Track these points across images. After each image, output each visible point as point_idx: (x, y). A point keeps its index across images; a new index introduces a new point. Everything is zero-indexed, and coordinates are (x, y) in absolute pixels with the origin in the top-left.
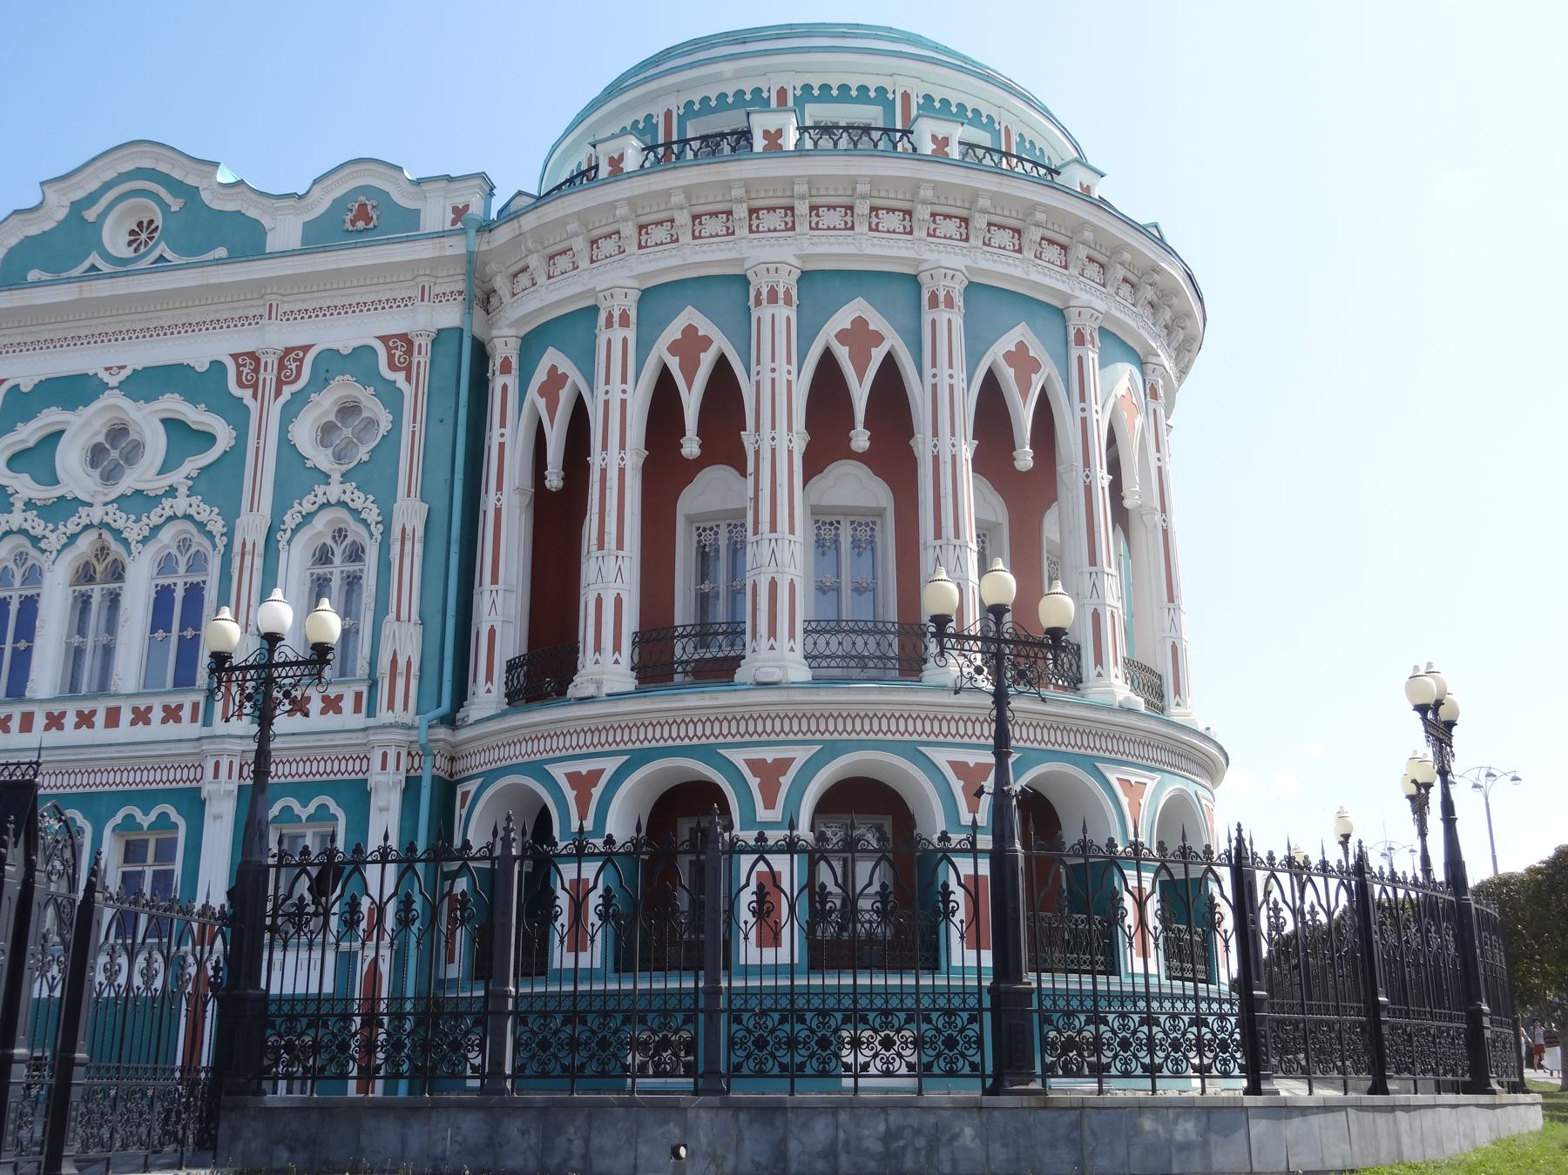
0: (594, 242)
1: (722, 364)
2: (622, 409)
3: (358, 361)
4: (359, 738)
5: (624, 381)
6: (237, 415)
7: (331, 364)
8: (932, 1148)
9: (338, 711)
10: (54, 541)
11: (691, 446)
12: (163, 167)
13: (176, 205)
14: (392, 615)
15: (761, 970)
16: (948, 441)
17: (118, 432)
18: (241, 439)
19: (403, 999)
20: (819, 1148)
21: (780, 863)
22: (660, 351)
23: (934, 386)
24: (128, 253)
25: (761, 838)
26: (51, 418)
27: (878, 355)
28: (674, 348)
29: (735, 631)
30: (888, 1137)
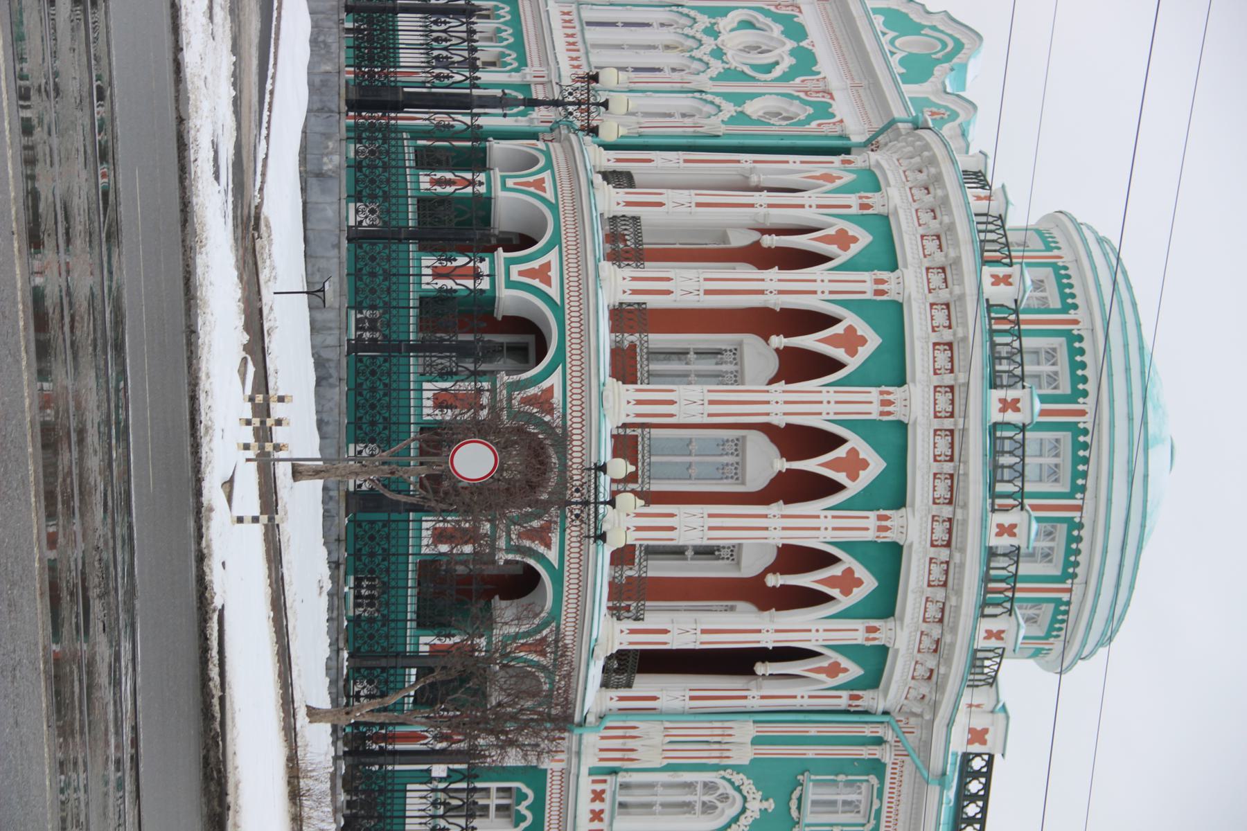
11: (778, 341)
23: (818, 517)
27: (840, 477)
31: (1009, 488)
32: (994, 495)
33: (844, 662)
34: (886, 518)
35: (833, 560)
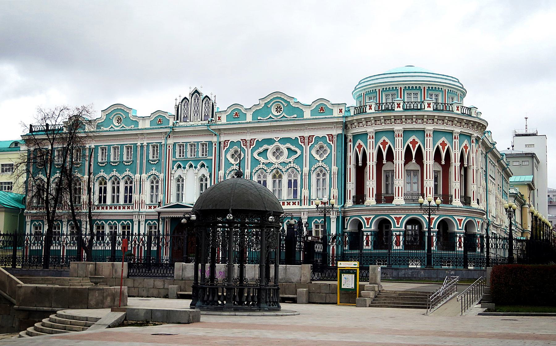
0: (367, 122)
1: (390, 146)
2: (372, 153)
6: (301, 148)
8: (418, 274)
10: (269, 171)
14: (332, 188)
16: (429, 161)
18: (302, 153)
22: (379, 144)
26: (265, 147)
27: (417, 146)
29: (392, 193)
30: (412, 273)
31: (419, 105)
32: (421, 109)
34: (427, 135)
35: (438, 147)
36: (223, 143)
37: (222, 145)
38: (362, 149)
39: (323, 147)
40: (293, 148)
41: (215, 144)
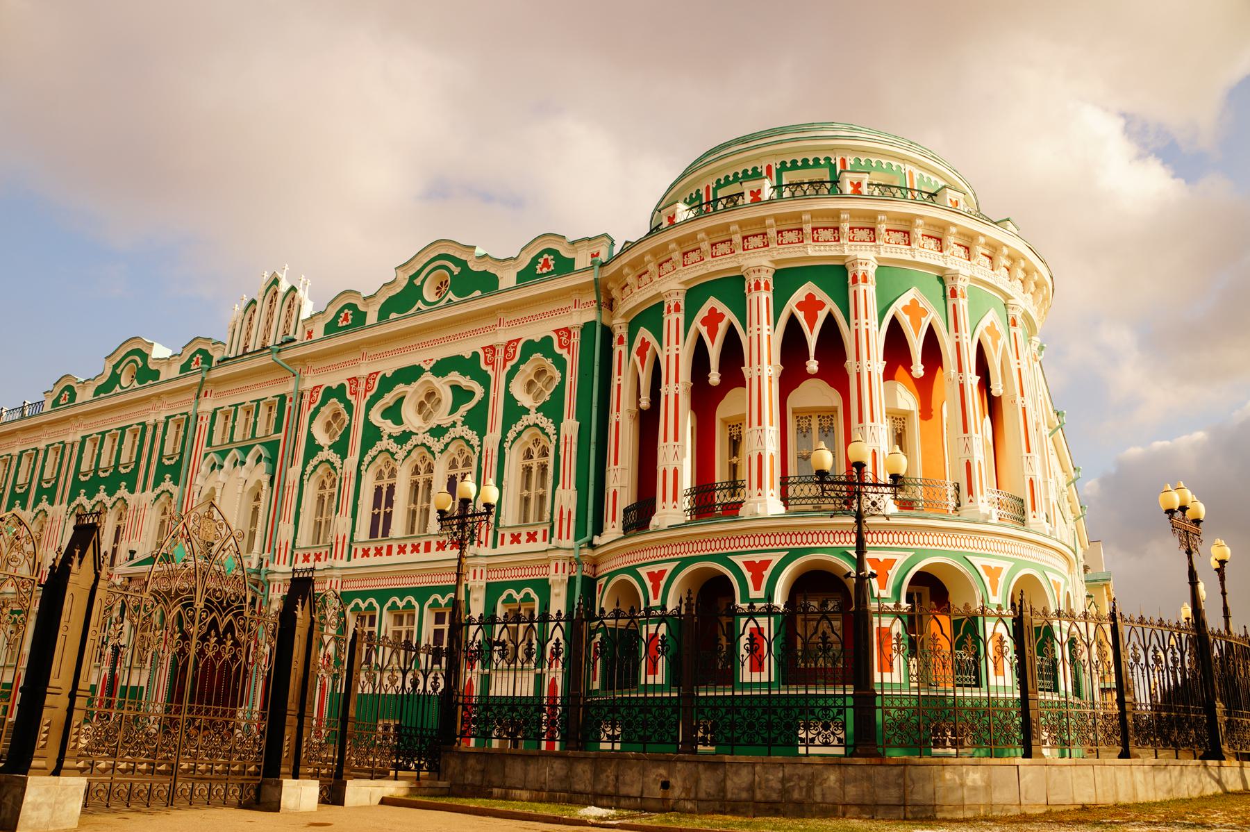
1: (731, 328)
3: (544, 346)
4: (543, 556)
5: (677, 343)
6: (484, 380)
7: (530, 348)
8: (810, 789)
9: (535, 540)
10: (401, 455)
11: (714, 378)
12: (451, 252)
13: (456, 271)
15: (751, 685)
17: (430, 395)
19: (541, 698)
20: (744, 785)
21: (763, 622)
22: (697, 323)
24: (437, 299)
25: (752, 606)
26: (400, 388)
27: (822, 316)
28: (704, 322)
30: (783, 780)
33: (985, 323)
36: (307, 394)
37: (306, 400)
38: (648, 353)
39: (544, 371)
40: (466, 382)
41: (291, 400)
